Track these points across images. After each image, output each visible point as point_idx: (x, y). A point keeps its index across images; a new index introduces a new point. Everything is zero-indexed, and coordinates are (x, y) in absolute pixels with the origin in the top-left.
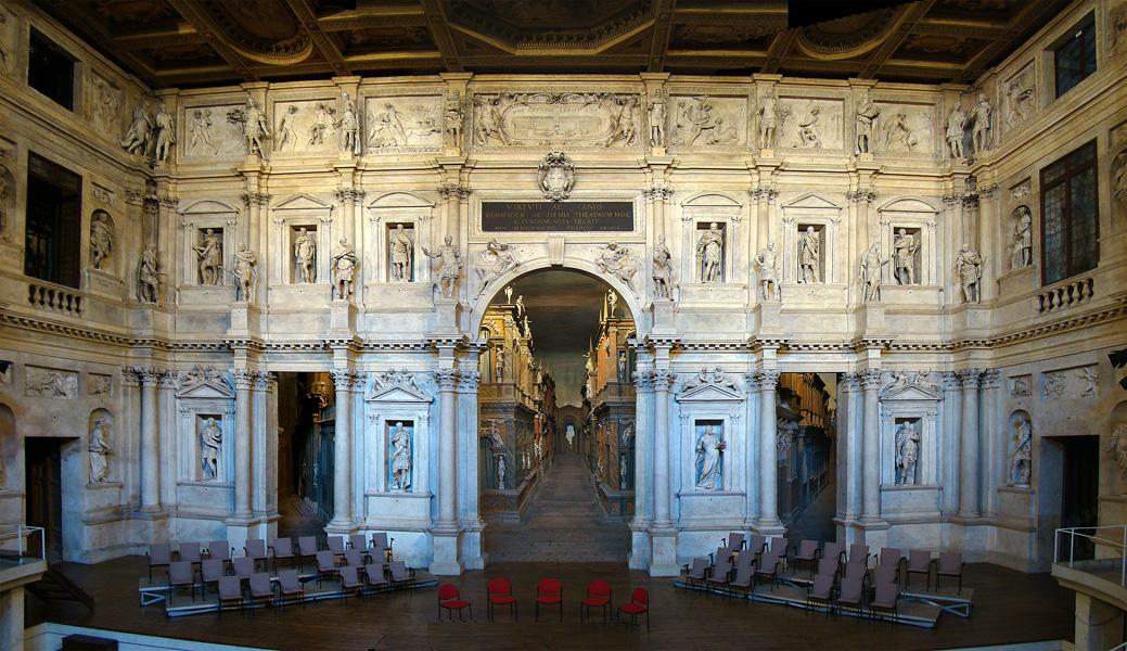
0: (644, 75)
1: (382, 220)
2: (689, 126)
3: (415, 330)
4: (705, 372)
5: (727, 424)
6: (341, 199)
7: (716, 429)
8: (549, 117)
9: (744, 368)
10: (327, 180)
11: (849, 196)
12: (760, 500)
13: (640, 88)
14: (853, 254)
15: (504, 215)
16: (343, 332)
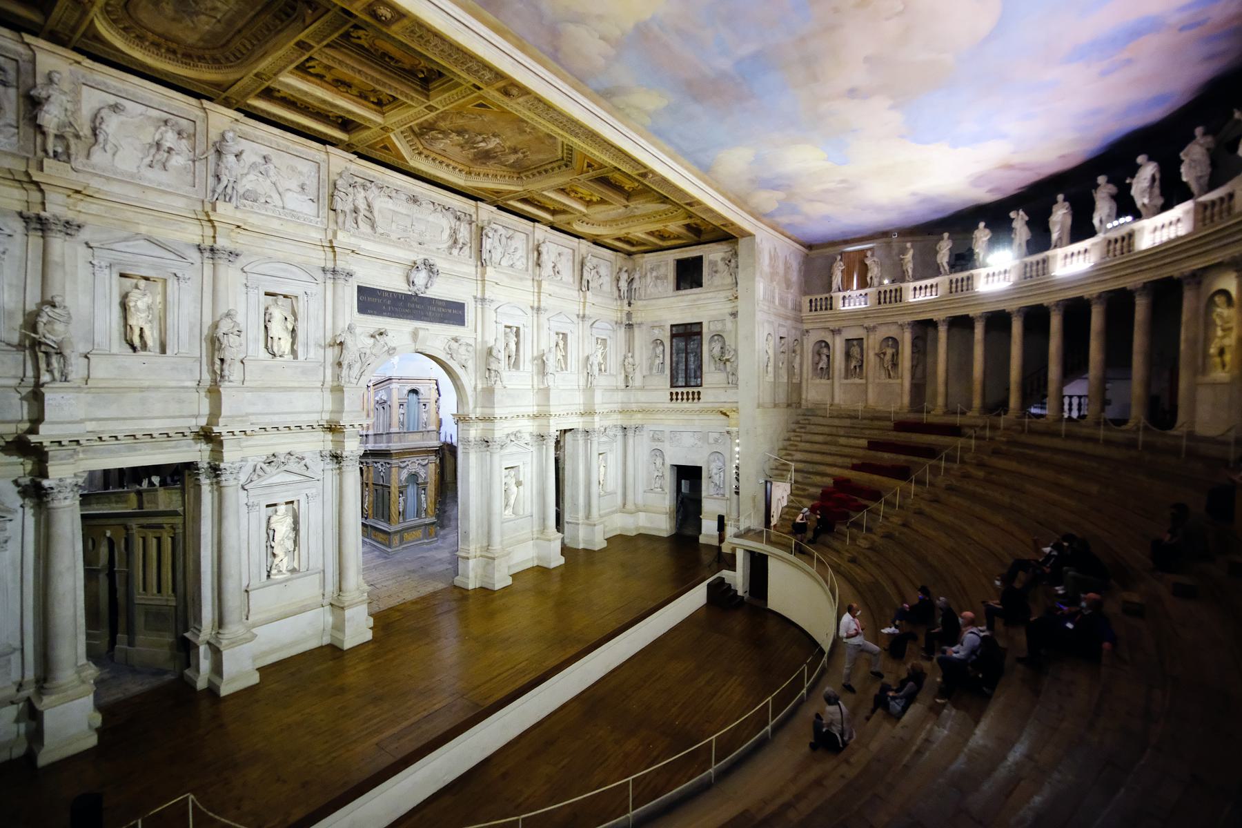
0: (480, 203)
1: (260, 288)
2: (500, 250)
3: (302, 410)
4: (512, 433)
5: (521, 469)
6: (207, 254)
7: (512, 472)
8: (408, 216)
9: (531, 429)
10: (186, 225)
11: (578, 316)
12: (544, 519)
13: (472, 211)
14: (581, 354)
15: (375, 300)
16: (241, 421)
